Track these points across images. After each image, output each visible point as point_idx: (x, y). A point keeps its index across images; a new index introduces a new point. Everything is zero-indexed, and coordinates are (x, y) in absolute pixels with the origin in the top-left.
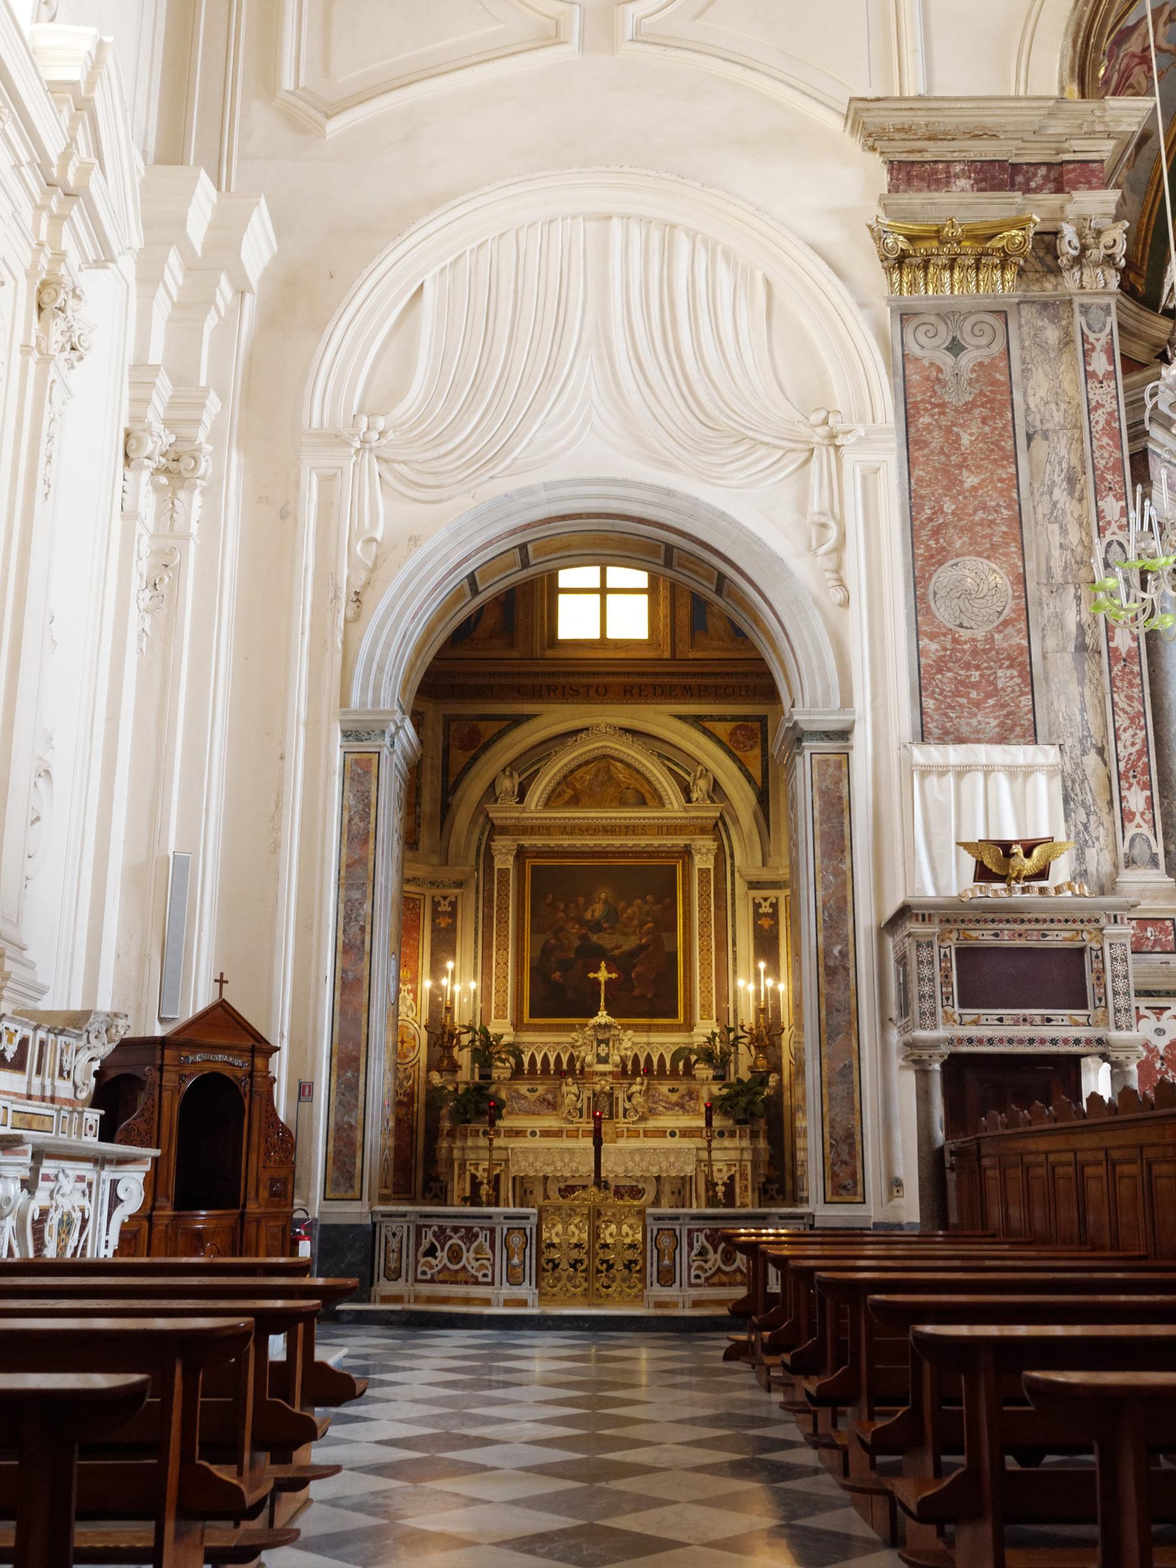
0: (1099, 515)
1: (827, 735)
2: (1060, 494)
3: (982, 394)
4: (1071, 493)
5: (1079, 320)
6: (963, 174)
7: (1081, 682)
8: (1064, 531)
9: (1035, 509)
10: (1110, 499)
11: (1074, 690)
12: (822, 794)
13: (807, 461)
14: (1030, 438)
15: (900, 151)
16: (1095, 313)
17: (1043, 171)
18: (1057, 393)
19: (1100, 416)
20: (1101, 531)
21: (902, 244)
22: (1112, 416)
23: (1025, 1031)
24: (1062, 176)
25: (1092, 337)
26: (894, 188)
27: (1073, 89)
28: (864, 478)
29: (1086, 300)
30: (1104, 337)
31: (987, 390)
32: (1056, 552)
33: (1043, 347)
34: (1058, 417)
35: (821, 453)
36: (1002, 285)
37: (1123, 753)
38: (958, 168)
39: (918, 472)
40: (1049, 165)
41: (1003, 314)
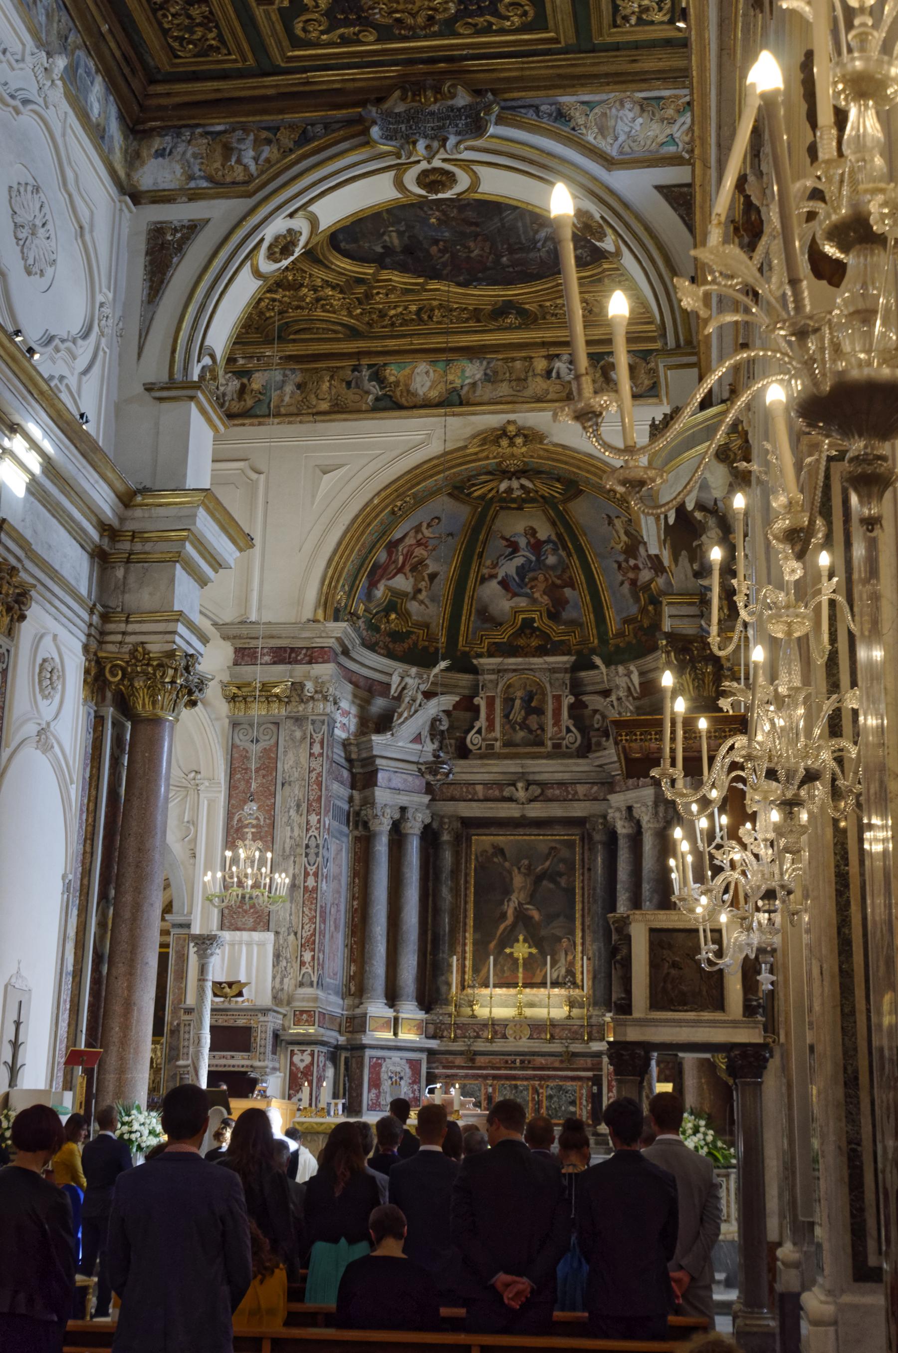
0: (308, 822)
1: (181, 926)
2: (292, 812)
3: (264, 764)
4: (297, 811)
5: (310, 727)
6: (268, 654)
7: (291, 902)
8: (292, 830)
9: (280, 819)
10: (314, 815)
11: (288, 905)
12: (177, 952)
13: (186, 796)
14: (283, 785)
15: (240, 644)
16: (318, 724)
17: (304, 651)
18: (297, 763)
19: (314, 775)
20: (307, 830)
21: (235, 690)
22: (320, 775)
23: (223, 1062)
24: (314, 655)
25: (315, 736)
26: (236, 664)
27: (320, 613)
28: (209, 805)
29: (314, 718)
30: (320, 736)
31: (267, 761)
32: (288, 840)
33: (293, 739)
34: (296, 775)
35: (191, 792)
36: (277, 710)
37: (304, 935)
38: (265, 651)
39: (233, 802)
40: (308, 648)
41: (277, 724)
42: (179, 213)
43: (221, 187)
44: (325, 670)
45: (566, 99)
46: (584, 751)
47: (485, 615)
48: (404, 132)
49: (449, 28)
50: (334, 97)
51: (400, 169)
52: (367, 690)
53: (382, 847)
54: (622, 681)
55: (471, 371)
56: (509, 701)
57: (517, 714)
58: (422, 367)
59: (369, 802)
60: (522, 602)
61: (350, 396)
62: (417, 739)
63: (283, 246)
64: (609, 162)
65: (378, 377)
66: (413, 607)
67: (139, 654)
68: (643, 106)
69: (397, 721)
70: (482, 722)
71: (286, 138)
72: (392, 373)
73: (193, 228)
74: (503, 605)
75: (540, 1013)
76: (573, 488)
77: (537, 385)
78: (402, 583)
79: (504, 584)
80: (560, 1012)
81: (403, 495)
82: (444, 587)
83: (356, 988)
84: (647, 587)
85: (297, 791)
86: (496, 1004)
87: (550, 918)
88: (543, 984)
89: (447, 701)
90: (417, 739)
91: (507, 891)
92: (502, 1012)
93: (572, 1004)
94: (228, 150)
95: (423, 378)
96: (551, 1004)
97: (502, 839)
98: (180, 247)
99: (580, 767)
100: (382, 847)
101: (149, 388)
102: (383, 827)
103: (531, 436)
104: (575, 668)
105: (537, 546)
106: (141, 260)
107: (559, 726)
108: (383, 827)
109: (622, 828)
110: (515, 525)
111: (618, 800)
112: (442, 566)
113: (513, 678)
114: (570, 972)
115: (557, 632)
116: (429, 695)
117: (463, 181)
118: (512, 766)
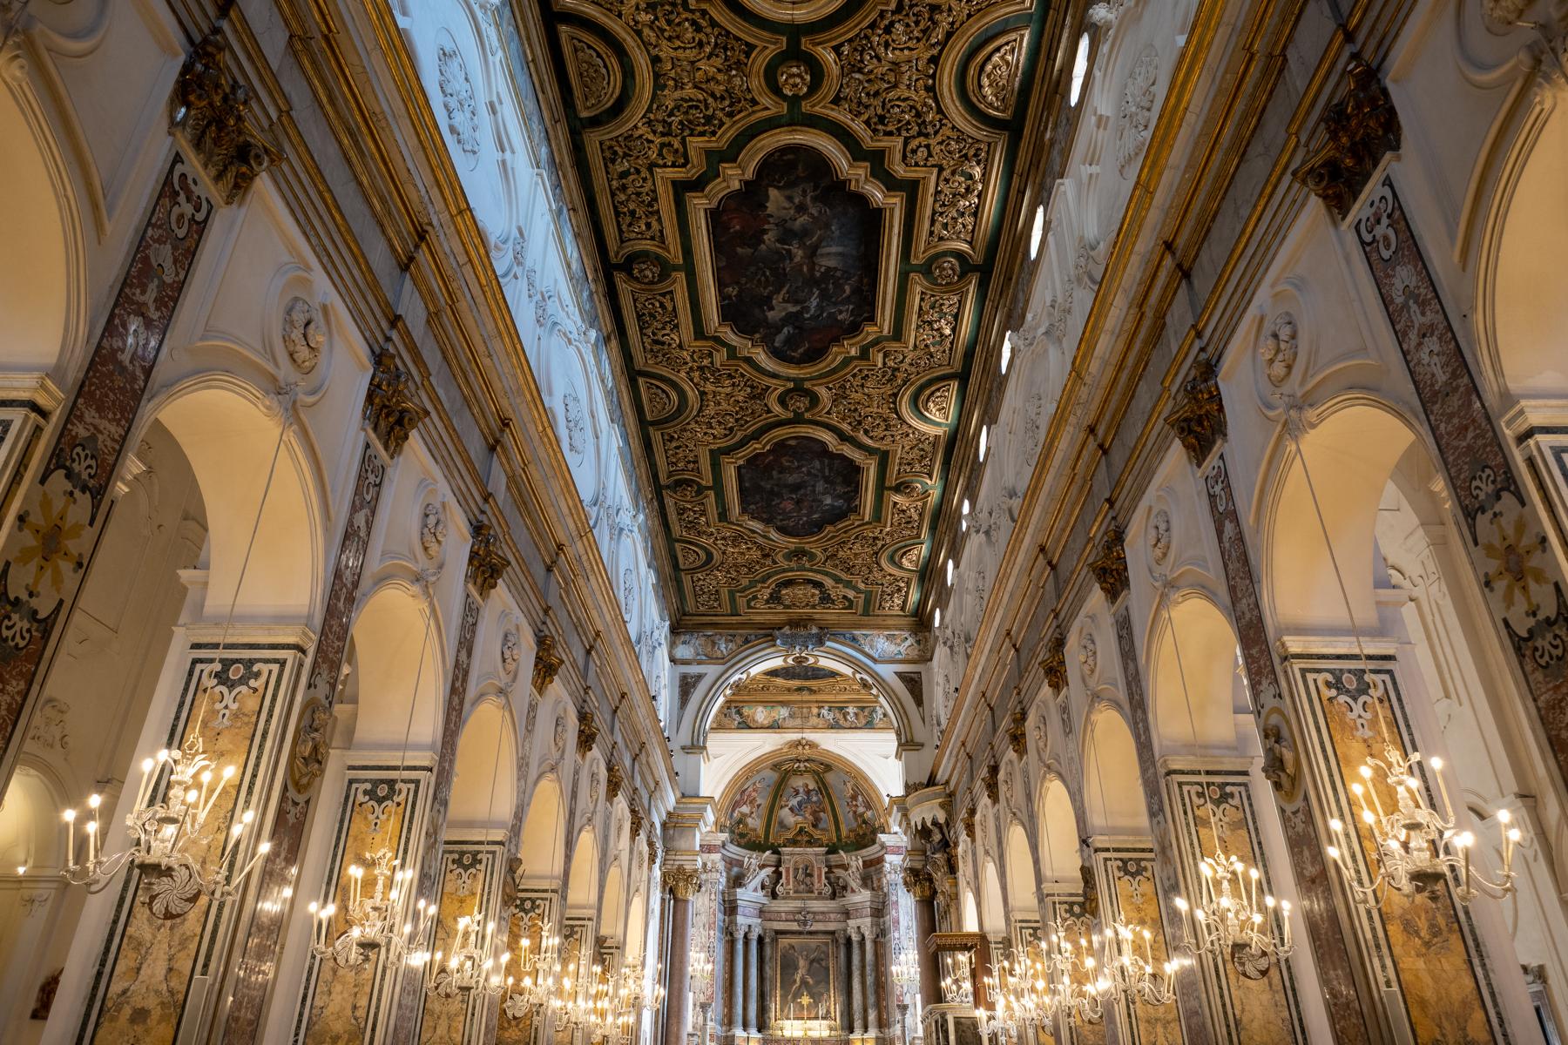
42: (694, 670)
43: (712, 659)
44: (716, 857)
45: (856, 632)
46: (833, 896)
47: (782, 824)
48: (790, 643)
49: (814, 607)
50: (761, 626)
51: (787, 656)
52: (730, 863)
53: (740, 946)
54: (853, 864)
55: (784, 712)
56: (796, 870)
57: (800, 876)
58: (760, 709)
59: (733, 922)
60: (800, 819)
61: (726, 721)
62: (755, 890)
63: (738, 687)
64: (875, 661)
65: (739, 713)
66: (749, 820)
67: (680, 869)
68: (888, 637)
69: (746, 881)
70: (783, 880)
71: (739, 641)
72: (746, 711)
73: (700, 677)
74: (791, 819)
75: (815, 1034)
76: (828, 768)
77: (814, 721)
78: (745, 809)
79: (791, 809)
80: (826, 1034)
81: (751, 770)
82: (764, 811)
83: (729, 1022)
84: (862, 815)
85: (703, 918)
86: (792, 1028)
87: (817, 983)
88: (816, 1018)
89: (769, 870)
90: (755, 890)
91: (797, 969)
92: (798, 1034)
93: (831, 1029)
94: (714, 643)
95: (761, 714)
96: (820, 1029)
97: (794, 941)
98: (694, 686)
99: (832, 904)
100: (740, 946)
101: (683, 748)
102: (740, 936)
103: (812, 745)
104: (828, 853)
105: (808, 792)
106: (677, 690)
107: (820, 884)
108: (740, 936)
109: (855, 938)
110: (798, 782)
111: (852, 923)
112: (763, 801)
113: (797, 858)
114: (828, 1012)
115: (817, 834)
116: (762, 867)
117: (812, 660)
118: (799, 904)
